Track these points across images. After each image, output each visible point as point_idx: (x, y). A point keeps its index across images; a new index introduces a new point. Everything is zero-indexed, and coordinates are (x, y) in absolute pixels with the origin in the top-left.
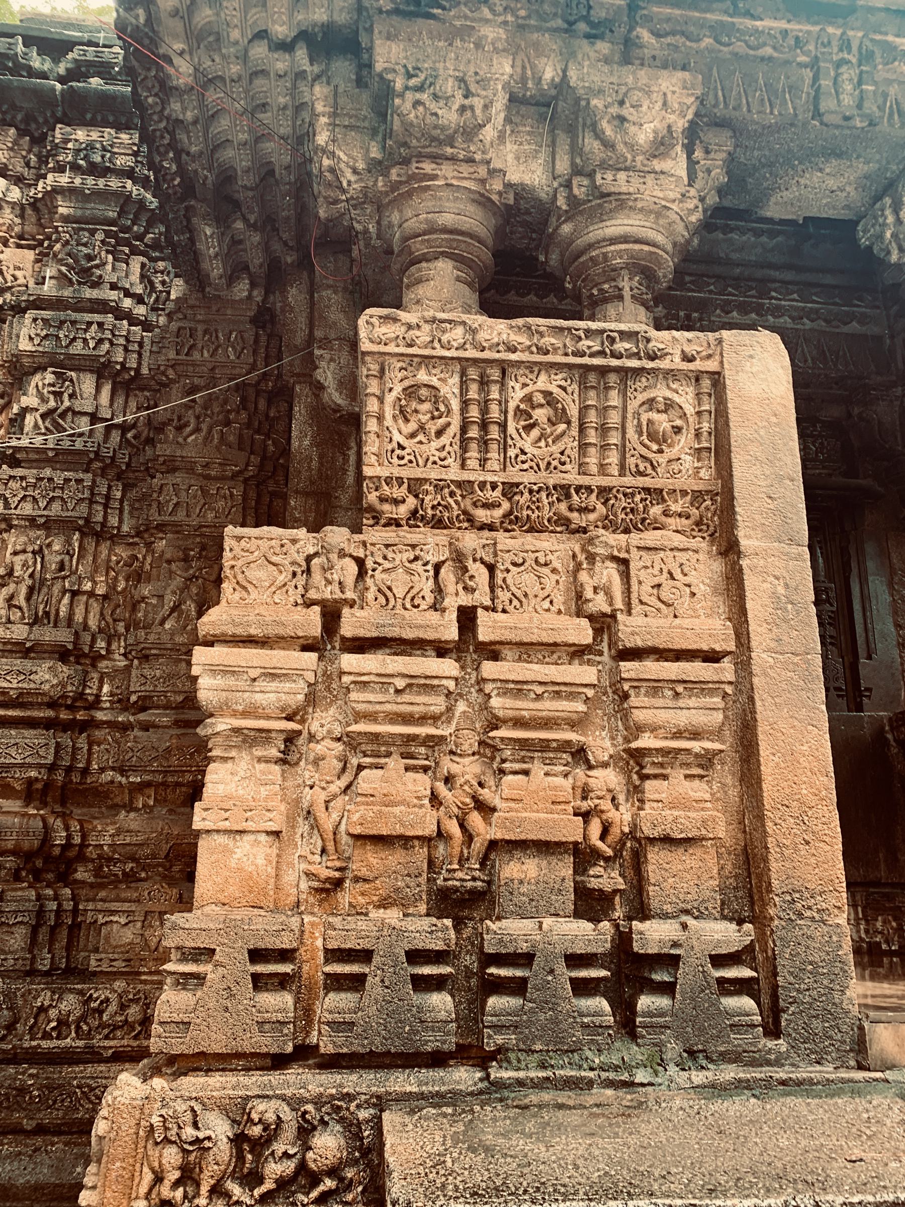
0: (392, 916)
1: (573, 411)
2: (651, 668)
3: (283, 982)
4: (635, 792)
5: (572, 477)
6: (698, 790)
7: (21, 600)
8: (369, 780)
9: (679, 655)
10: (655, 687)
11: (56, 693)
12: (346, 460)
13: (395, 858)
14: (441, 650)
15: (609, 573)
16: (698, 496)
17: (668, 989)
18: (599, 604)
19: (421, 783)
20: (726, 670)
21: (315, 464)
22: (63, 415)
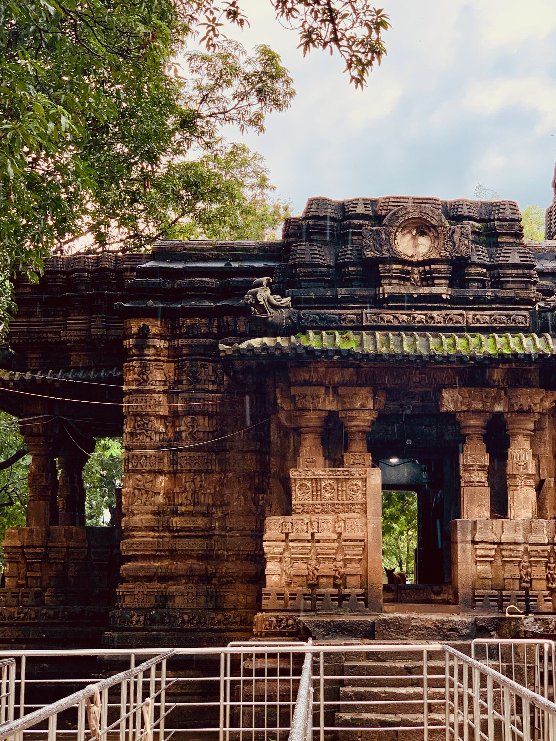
0: (300, 588)
1: (335, 487)
2: (348, 543)
3: (282, 599)
4: (345, 566)
5: (336, 501)
6: (357, 566)
7: (190, 497)
8: (295, 565)
9: (355, 540)
10: (349, 547)
11: (204, 527)
12: (289, 442)
13: (300, 579)
14: (308, 541)
15: (342, 523)
16: (362, 505)
17: (348, 600)
18: (339, 530)
19: (304, 566)
20: (363, 543)
21: (279, 445)
22: (195, 433)
